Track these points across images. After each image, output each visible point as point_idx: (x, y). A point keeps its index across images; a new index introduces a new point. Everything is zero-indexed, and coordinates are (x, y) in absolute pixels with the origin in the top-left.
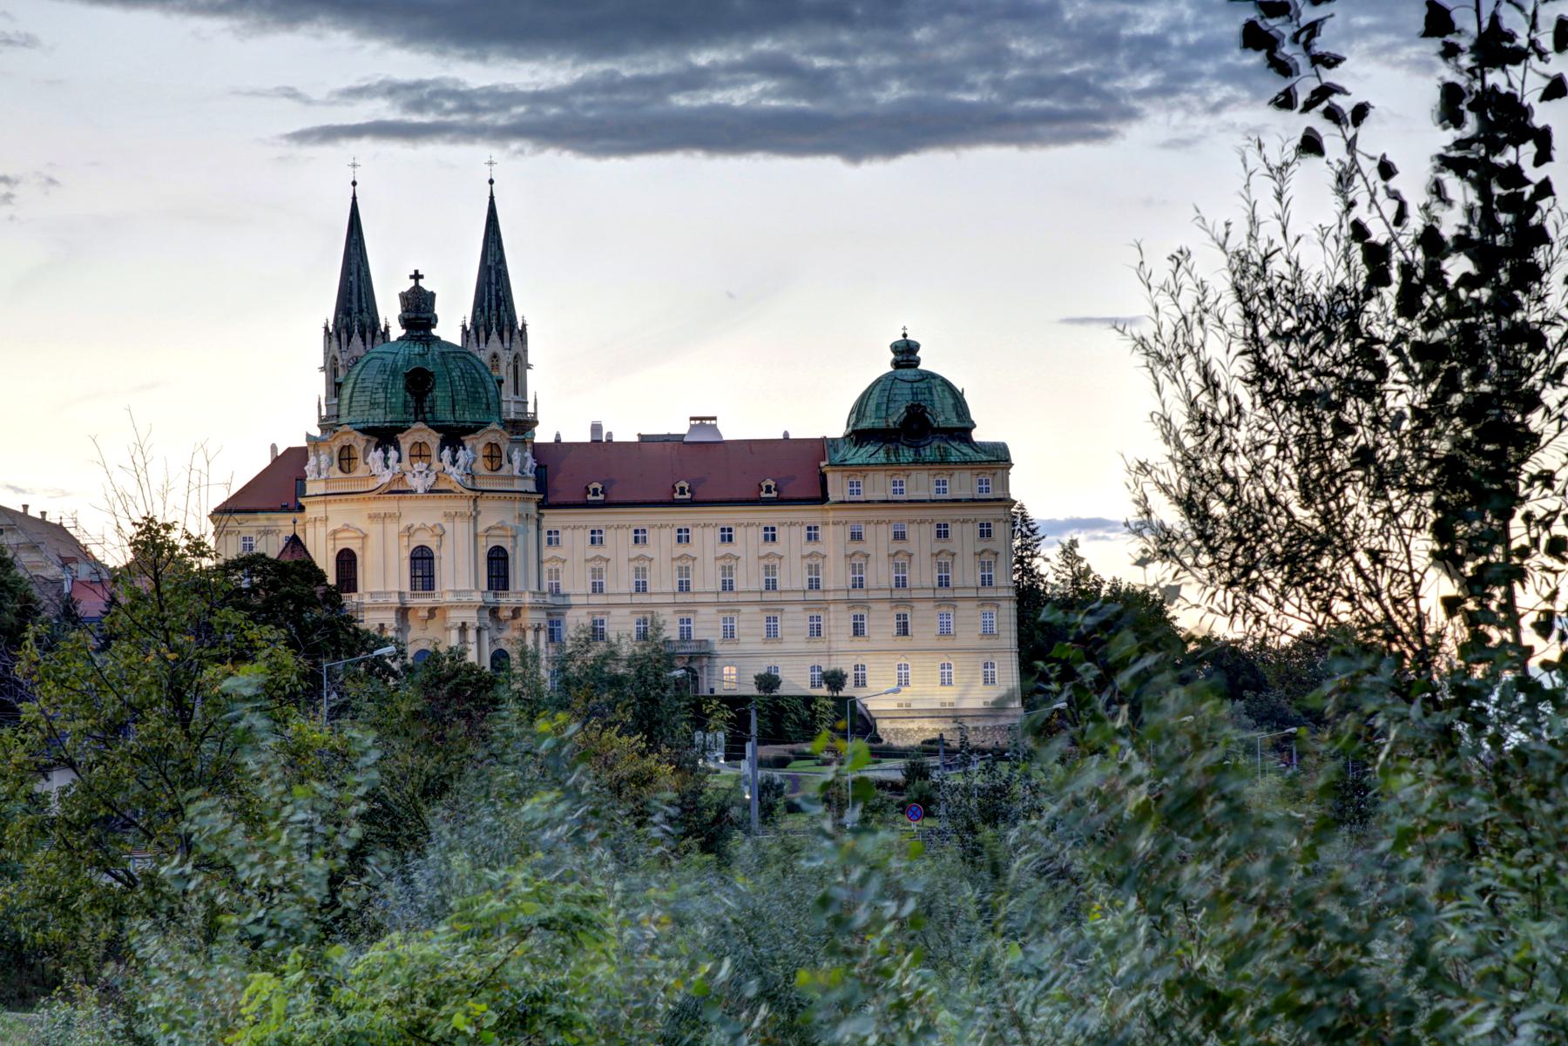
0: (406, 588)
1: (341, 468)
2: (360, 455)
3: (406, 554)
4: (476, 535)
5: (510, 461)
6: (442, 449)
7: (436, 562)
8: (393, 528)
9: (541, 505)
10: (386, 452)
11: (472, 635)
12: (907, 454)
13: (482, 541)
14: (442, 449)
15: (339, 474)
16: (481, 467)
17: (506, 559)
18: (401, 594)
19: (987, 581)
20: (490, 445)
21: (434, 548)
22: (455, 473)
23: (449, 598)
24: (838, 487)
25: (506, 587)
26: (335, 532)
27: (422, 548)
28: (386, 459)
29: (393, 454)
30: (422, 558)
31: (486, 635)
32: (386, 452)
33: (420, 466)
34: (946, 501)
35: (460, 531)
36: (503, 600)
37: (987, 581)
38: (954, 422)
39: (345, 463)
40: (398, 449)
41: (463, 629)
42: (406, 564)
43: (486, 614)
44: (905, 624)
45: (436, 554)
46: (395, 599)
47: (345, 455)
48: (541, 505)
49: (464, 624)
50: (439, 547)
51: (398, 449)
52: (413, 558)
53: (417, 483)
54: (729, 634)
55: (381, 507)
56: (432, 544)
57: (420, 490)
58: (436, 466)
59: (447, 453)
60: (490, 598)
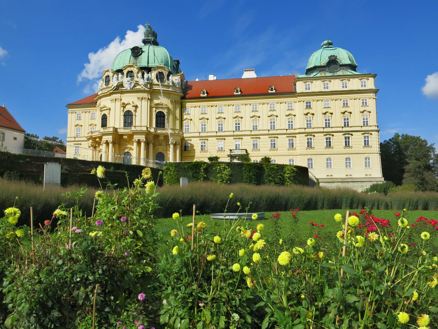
0: (122, 126)
1: (106, 85)
2: (111, 79)
3: (122, 114)
4: (151, 108)
5: (168, 79)
6: (138, 73)
7: (134, 117)
9: (183, 98)
10: (118, 75)
11: (143, 145)
13: (154, 109)
14: (138, 73)
15: (105, 87)
16: (155, 81)
17: (164, 116)
18: (115, 129)
19: (366, 123)
20: (159, 73)
21: (133, 111)
22: (141, 82)
24: (300, 87)
25: (164, 126)
26: (101, 108)
27: (129, 111)
29: (120, 75)
30: (128, 115)
31: (151, 146)
33: (129, 78)
35: (144, 106)
36: (159, 132)
37: (366, 123)
38: (348, 62)
39: (107, 83)
40: (123, 74)
41: (139, 142)
42: (122, 118)
43: (151, 138)
44: (330, 142)
45: (134, 113)
46: (111, 130)
47: (107, 80)
49: (139, 140)
50: (136, 111)
51: (123, 74)
52: (125, 116)
53: (127, 86)
54: (255, 146)
55: (114, 96)
56: (132, 109)
57: (129, 89)
58: (136, 79)
59: (140, 75)
60: (152, 130)
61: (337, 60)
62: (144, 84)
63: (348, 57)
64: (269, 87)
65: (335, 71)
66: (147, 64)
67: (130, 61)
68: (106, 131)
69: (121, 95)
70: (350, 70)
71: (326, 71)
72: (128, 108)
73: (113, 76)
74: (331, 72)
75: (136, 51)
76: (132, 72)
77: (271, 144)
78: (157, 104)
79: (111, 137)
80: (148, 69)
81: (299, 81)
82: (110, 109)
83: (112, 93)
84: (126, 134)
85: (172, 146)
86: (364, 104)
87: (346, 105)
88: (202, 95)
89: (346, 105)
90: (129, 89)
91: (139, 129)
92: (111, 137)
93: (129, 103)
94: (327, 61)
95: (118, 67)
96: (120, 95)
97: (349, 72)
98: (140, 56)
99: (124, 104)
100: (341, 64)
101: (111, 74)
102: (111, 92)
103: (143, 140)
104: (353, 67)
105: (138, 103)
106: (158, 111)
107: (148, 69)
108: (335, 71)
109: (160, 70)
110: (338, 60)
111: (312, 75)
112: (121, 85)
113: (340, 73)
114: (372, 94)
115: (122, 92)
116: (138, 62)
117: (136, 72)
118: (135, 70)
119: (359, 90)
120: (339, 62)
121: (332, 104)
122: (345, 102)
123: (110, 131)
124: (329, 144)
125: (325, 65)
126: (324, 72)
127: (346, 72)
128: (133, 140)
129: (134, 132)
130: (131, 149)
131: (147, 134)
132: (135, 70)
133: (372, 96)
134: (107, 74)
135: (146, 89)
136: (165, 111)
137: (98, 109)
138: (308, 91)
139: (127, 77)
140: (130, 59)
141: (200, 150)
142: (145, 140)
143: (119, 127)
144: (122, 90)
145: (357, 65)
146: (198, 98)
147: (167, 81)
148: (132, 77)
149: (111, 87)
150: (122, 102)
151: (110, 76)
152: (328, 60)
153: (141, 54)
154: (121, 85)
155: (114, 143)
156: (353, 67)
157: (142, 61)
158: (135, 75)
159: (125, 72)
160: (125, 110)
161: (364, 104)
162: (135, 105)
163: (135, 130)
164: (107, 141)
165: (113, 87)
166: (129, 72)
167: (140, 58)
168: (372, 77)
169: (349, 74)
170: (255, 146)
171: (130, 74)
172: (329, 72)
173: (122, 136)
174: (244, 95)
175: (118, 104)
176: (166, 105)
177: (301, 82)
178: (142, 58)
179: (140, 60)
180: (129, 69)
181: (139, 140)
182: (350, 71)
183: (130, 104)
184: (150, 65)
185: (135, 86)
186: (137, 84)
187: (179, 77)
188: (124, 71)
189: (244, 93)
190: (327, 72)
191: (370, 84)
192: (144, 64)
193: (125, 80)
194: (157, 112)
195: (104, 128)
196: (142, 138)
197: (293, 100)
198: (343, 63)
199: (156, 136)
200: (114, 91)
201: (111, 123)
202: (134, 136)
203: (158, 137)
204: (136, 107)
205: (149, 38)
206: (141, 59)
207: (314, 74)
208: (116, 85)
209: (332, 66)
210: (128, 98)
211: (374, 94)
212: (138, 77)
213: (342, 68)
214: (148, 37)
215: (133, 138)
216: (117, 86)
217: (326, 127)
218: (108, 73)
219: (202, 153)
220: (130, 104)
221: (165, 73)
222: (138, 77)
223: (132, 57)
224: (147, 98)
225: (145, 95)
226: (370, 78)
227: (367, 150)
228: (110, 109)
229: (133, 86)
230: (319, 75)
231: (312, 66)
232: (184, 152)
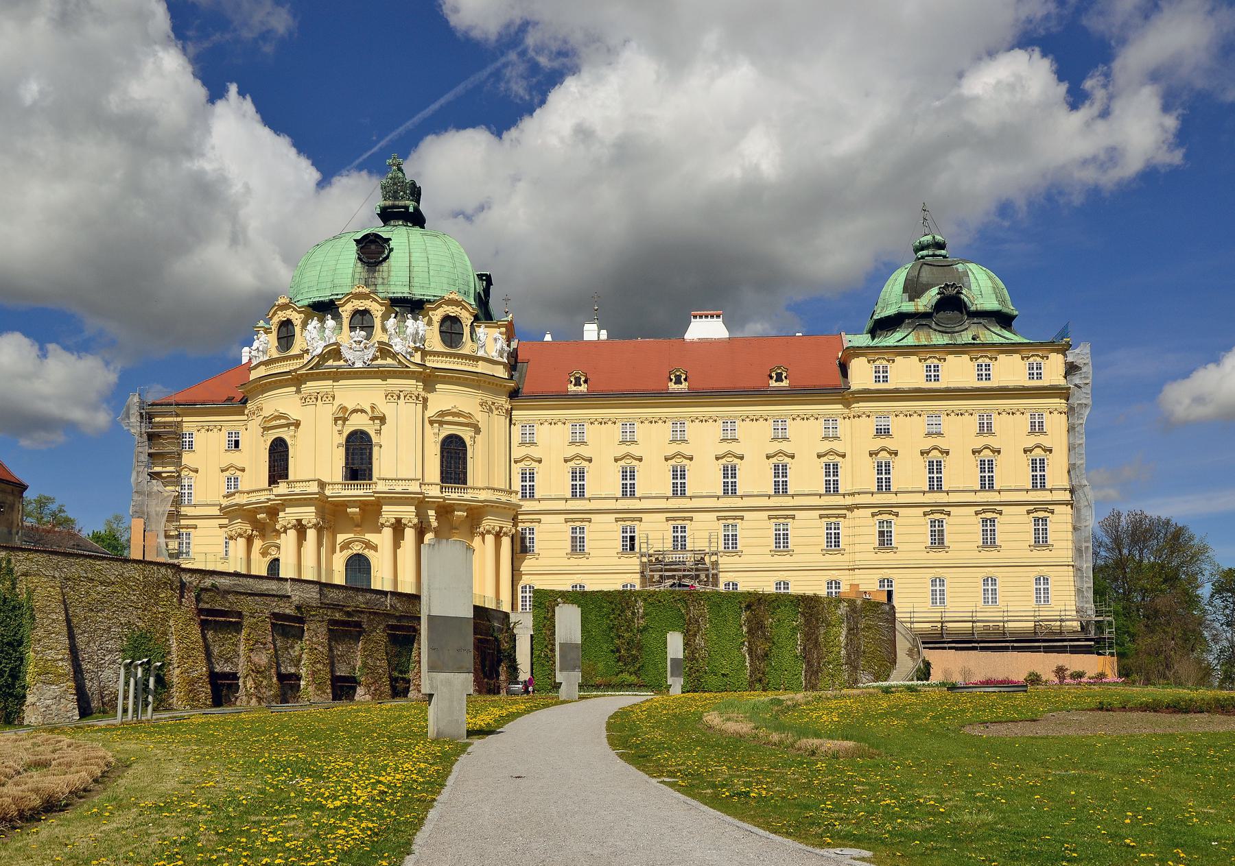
2: (297, 329)
6: (385, 317)
7: (375, 449)
8: (326, 412)
10: (322, 321)
11: (410, 534)
12: (939, 339)
14: (385, 317)
18: (322, 485)
23: (381, 487)
24: (861, 374)
28: (323, 329)
29: (330, 323)
32: (322, 321)
34: (992, 389)
36: (454, 496)
38: (991, 304)
40: (337, 316)
45: (375, 440)
46: (314, 488)
48: (514, 394)
49: (398, 521)
50: (379, 432)
51: (337, 316)
55: (310, 387)
58: (378, 335)
60: (434, 491)
61: (962, 296)
62: (407, 353)
63: (990, 291)
64: (771, 371)
65: (957, 329)
66: (406, 290)
67: (353, 276)
68: (297, 491)
69: (335, 384)
70: (999, 328)
71: (930, 327)
72: (358, 422)
73: (304, 324)
74: (946, 333)
75: (373, 247)
76: (365, 312)
77: (777, 536)
78: (443, 413)
79: (312, 509)
80: (413, 306)
81: (858, 356)
82: (297, 424)
83: (307, 374)
84: (354, 501)
85: (490, 539)
86: (1037, 428)
87: (985, 428)
88: (572, 388)
89: (985, 428)
90: (359, 364)
91: (399, 489)
92: (312, 509)
93: (359, 407)
94: (934, 301)
95: (316, 294)
96: (330, 382)
97: (995, 334)
98: (385, 264)
99: (344, 409)
100: (973, 308)
101: (297, 318)
102: (303, 371)
103: (410, 521)
104: (1003, 319)
105: (385, 408)
106: (444, 433)
107: (413, 306)
108: (957, 329)
109: (452, 311)
110: (966, 299)
111: (892, 339)
112: (335, 352)
113: (966, 337)
114: (1058, 400)
115: (337, 376)
116: (380, 281)
117: (380, 314)
118: (377, 310)
119: (1024, 388)
120: (968, 303)
121: (950, 425)
122: (985, 422)
123: (309, 490)
124: (938, 539)
125: (929, 310)
126: (926, 330)
127: (987, 332)
128: (382, 520)
129: (383, 497)
130: (368, 545)
131: (421, 504)
132: (377, 310)
133: (1058, 406)
134: (282, 316)
135: (413, 368)
136: (466, 434)
137: (255, 425)
138: (882, 386)
139: (352, 328)
140: (354, 272)
141: (569, 550)
142: (415, 521)
143: (330, 481)
144: (340, 367)
145: (1016, 313)
146: (561, 398)
147: (469, 343)
148: (369, 328)
149: (300, 356)
150: (337, 403)
151: (295, 322)
152: (939, 296)
153: (387, 257)
154: (335, 352)
155: (320, 530)
156: (1003, 319)
157: (393, 280)
158: (377, 322)
159: (346, 311)
160: (348, 430)
161: (1037, 428)
162: (376, 414)
163: (386, 489)
164: (299, 521)
165: (307, 358)
166: (356, 312)
167: (385, 269)
168: (1058, 352)
169: (997, 339)
170: (731, 541)
171: (362, 320)
172: (940, 331)
173: (343, 505)
174: (701, 395)
175: (326, 412)
176: (470, 416)
177: (863, 360)
178: (392, 269)
179: (385, 275)
180: (360, 305)
181: (398, 521)
182: (997, 329)
183: (363, 411)
184: (418, 294)
185: (375, 358)
186: (385, 350)
187: (503, 330)
188: (340, 310)
189: (700, 385)
190: (935, 330)
191: (1053, 370)
192: (401, 291)
193: (347, 339)
194: (442, 436)
195: (287, 482)
196: (408, 513)
197: (840, 412)
198: (979, 308)
199: (445, 510)
200: (312, 368)
201: (298, 466)
202: (385, 508)
203: (447, 512)
204: (383, 420)
205: (402, 203)
206: (389, 272)
207: (898, 335)
208: (319, 351)
209: (949, 314)
210: (353, 394)
211: (1063, 401)
212: (384, 330)
213: (975, 320)
214: (396, 198)
215: (379, 513)
216: (323, 357)
217: (931, 489)
218: (289, 312)
219: (573, 561)
220: (363, 411)
221: (466, 318)
222: (384, 330)
223: (359, 264)
224: (416, 393)
225: (410, 385)
226: (1053, 356)
227: (1041, 555)
228: (297, 424)
229: (370, 353)
230: (910, 340)
231: (891, 311)
232: (519, 556)
